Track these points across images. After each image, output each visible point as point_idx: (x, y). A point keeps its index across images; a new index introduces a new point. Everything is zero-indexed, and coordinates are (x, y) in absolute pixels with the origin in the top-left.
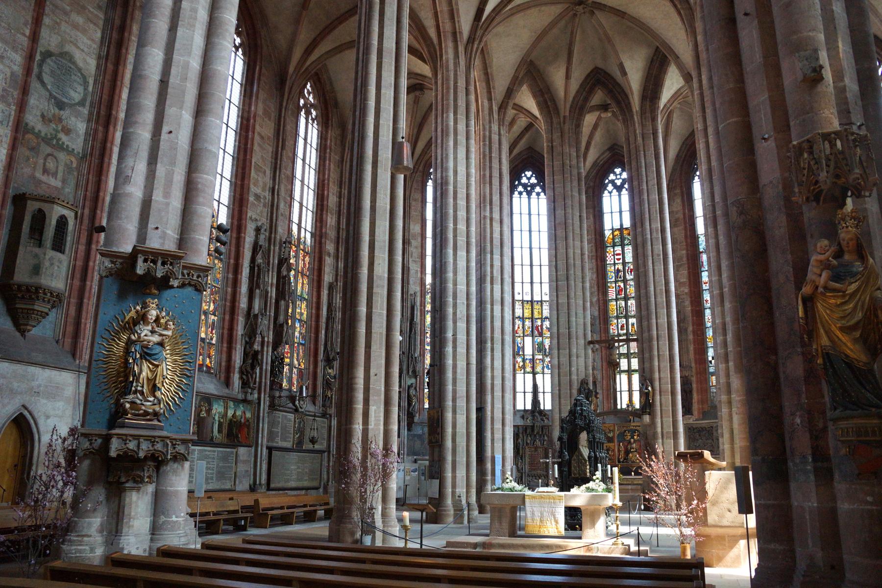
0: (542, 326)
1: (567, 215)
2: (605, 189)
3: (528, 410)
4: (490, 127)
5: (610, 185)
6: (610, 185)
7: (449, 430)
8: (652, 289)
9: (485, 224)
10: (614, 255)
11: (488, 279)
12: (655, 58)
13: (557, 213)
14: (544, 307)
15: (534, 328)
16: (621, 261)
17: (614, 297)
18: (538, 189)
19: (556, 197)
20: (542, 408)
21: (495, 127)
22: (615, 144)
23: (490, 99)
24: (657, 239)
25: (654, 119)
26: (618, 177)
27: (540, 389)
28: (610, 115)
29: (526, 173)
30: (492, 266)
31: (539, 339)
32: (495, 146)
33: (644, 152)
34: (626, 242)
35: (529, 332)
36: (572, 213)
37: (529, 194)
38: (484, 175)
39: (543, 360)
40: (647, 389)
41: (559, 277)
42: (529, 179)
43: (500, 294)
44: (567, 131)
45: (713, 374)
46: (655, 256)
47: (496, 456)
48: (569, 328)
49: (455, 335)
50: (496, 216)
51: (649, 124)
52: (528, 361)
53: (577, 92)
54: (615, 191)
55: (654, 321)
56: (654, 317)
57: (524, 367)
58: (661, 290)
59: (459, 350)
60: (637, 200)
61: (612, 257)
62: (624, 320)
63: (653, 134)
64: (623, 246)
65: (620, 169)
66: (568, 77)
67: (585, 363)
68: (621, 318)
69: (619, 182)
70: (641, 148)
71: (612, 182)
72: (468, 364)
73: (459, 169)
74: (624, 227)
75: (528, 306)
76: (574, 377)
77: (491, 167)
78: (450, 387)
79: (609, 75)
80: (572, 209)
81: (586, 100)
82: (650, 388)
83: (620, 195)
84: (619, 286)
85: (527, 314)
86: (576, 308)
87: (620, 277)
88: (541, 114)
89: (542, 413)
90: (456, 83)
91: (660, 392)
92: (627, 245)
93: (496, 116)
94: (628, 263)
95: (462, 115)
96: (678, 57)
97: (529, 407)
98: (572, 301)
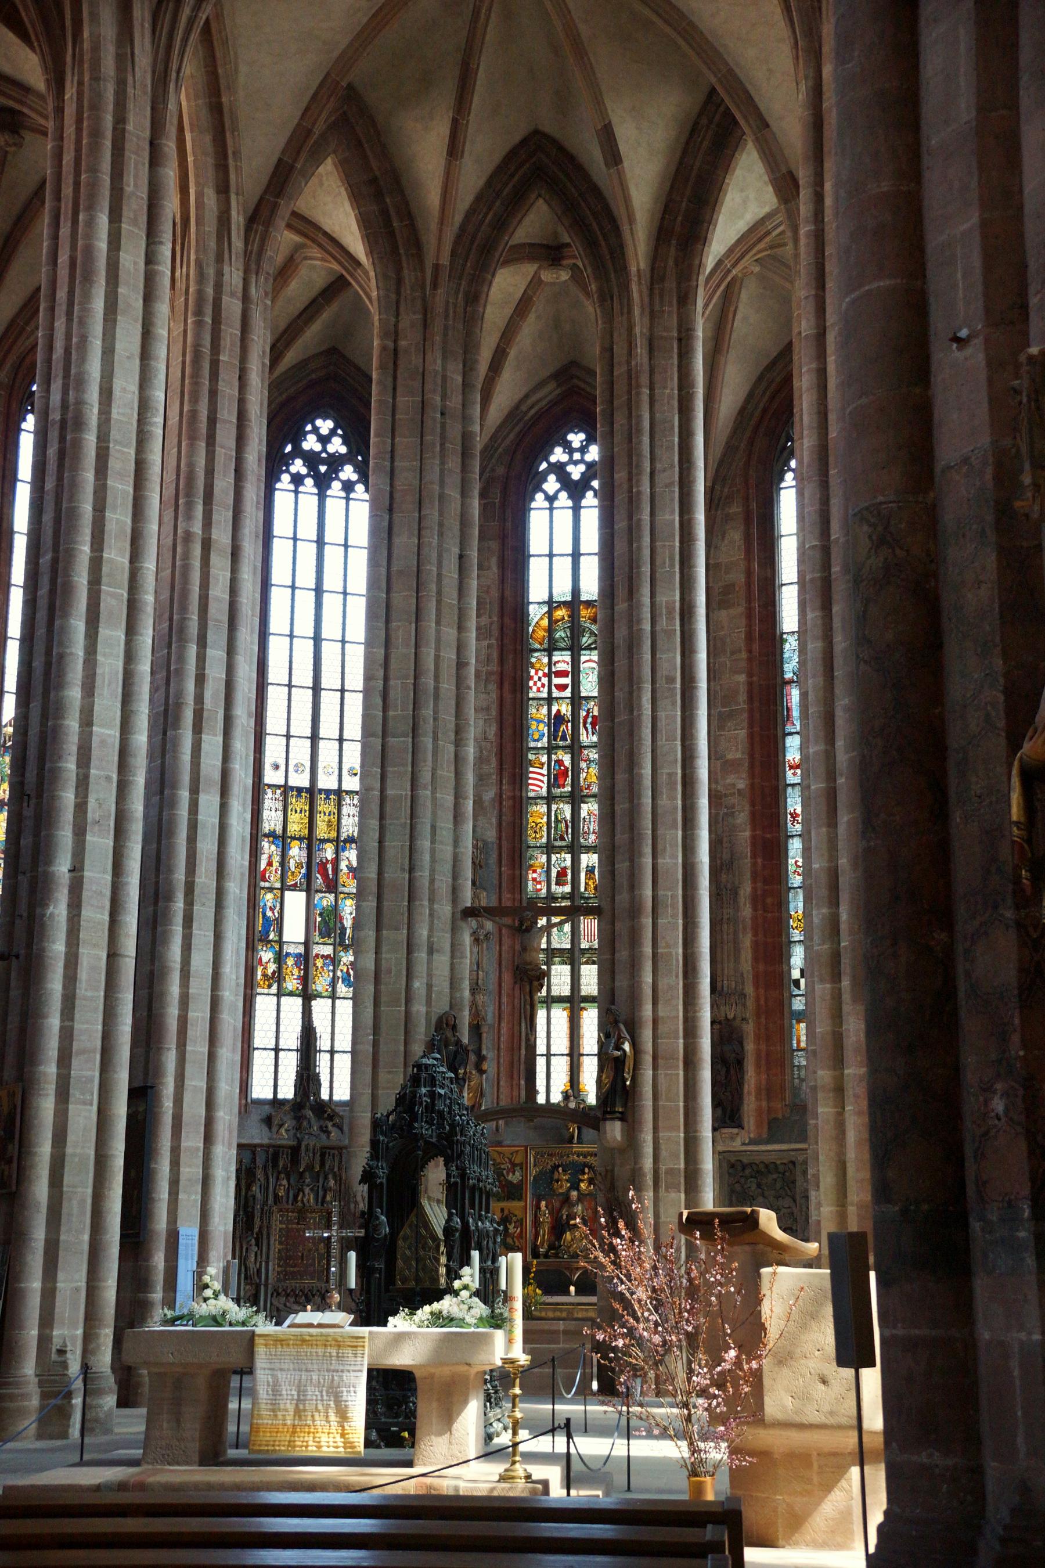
0: (336, 861)
1: (425, 551)
2: (538, 488)
3: (284, 1102)
4: (220, 274)
5: (552, 478)
6: (552, 478)
7: (44, 1149)
8: (647, 771)
9: (186, 556)
10: (549, 675)
11: (188, 715)
12: (704, 121)
13: (396, 541)
14: (345, 810)
15: (315, 868)
16: (568, 693)
17: (544, 792)
18: (348, 473)
19: (397, 496)
20: (325, 1095)
21: (234, 277)
22: (574, 364)
23: (223, 189)
24: (670, 633)
25: (685, 299)
26: (577, 456)
27: (323, 1043)
28: (564, 276)
29: (319, 422)
30: (201, 679)
31: (327, 900)
32: (231, 332)
33: (652, 389)
34: (585, 640)
35: (297, 876)
36: (440, 545)
37: (322, 484)
38: (194, 414)
39: (334, 960)
40: (618, 1047)
41: (391, 723)
42: (324, 440)
43: (219, 763)
44: (439, 309)
45: (800, 1017)
46: (661, 683)
47: (183, 1231)
48: (411, 870)
49: (77, 869)
50: (222, 536)
51: (670, 311)
52: (290, 961)
53: (479, 198)
54: (563, 495)
55: (648, 860)
56: (648, 850)
57: (278, 977)
58: (671, 775)
59: (86, 913)
60: (621, 525)
61: (545, 680)
62: (568, 857)
63: (680, 340)
64: (575, 650)
65: (582, 436)
66: (454, 150)
67: (452, 965)
68: (559, 850)
69: (576, 472)
70: (644, 379)
71: (559, 469)
72: (113, 955)
73: (118, 384)
74: (583, 598)
75: (299, 804)
76: (419, 1008)
77: (213, 393)
78: (54, 1022)
79: (571, 158)
80: (441, 534)
81: (502, 225)
82: (627, 1047)
83: (576, 509)
84: (560, 762)
85: (297, 825)
86: (434, 814)
87: (564, 738)
88: (371, 252)
89: (326, 1111)
90: (120, 120)
91: (655, 1058)
92: (589, 648)
93: (238, 244)
94: (587, 698)
95: (135, 222)
96: (767, 126)
97: (287, 1091)
98: (425, 793)
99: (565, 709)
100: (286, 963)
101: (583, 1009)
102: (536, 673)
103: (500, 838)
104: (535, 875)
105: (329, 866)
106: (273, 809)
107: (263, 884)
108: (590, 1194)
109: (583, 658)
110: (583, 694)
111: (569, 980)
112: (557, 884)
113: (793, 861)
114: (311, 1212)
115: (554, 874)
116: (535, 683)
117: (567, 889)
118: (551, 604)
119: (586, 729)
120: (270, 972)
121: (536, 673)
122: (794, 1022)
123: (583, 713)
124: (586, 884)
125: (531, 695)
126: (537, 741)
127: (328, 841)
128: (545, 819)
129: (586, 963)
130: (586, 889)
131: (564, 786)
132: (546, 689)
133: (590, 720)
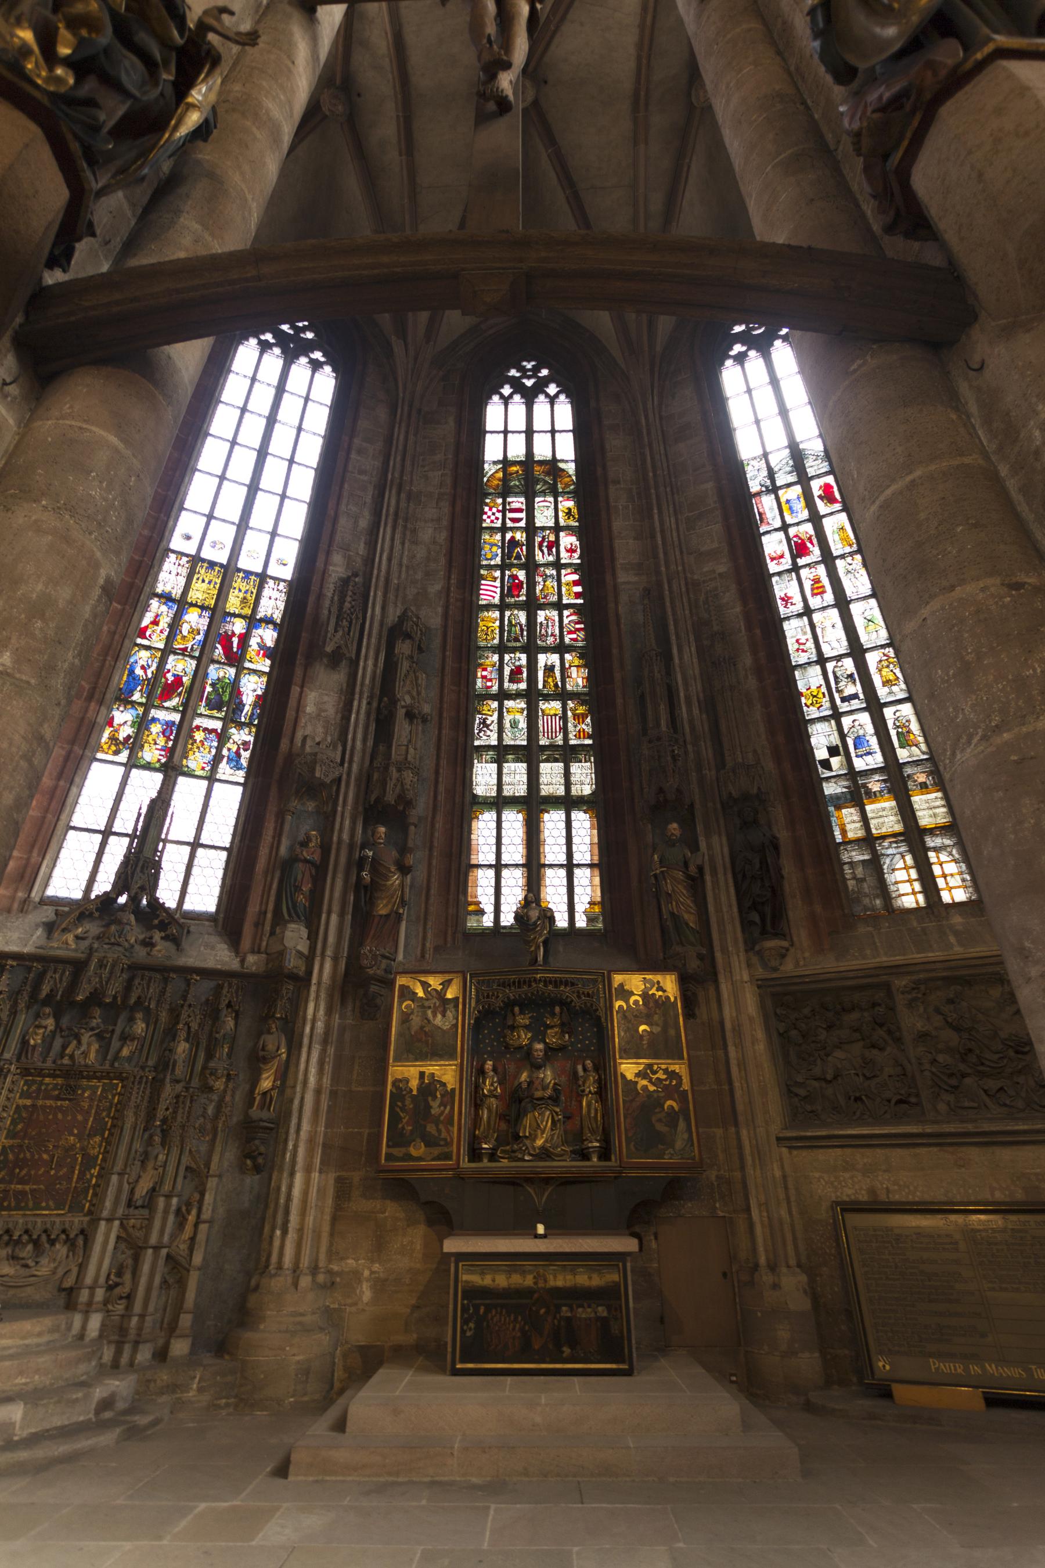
0: (244, 638)
16: (523, 524)
17: (497, 601)
39: (222, 737)
45: (839, 802)
52: (156, 728)
57: (134, 744)
68: (513, 650)
84: (516, 577)
87: (518, 557)
92: (544, 493)
94: (543, 528)
99: (520, 536)
100: (148, 729)
102: (490, 509)
103: (445, 627)
104: (485, 673)
105: (235, 640)
106: (174, 573)
107: (139, 641)
108: (562, 1048)
109: (537, 500)
110: (538, 524)
111: (525, 778)
112: (510, 681)
113: (794, 640)
114: (89, 1078)
115: (507, 671)
116: (489, 517)
117: (523, 686)
118: (506, 463)
119: (542, 551)
120: (122, 736)
121: (490, 509)
123: (538, 539)
124: (544, 681)
125: (484, 525)
126: (491, 559)
127: (239, 616)
128: (498, 623)
129: (547, 761)
130: (544, 686)
131: (518, 596)
132: (500, 521)
133: (545, 544)
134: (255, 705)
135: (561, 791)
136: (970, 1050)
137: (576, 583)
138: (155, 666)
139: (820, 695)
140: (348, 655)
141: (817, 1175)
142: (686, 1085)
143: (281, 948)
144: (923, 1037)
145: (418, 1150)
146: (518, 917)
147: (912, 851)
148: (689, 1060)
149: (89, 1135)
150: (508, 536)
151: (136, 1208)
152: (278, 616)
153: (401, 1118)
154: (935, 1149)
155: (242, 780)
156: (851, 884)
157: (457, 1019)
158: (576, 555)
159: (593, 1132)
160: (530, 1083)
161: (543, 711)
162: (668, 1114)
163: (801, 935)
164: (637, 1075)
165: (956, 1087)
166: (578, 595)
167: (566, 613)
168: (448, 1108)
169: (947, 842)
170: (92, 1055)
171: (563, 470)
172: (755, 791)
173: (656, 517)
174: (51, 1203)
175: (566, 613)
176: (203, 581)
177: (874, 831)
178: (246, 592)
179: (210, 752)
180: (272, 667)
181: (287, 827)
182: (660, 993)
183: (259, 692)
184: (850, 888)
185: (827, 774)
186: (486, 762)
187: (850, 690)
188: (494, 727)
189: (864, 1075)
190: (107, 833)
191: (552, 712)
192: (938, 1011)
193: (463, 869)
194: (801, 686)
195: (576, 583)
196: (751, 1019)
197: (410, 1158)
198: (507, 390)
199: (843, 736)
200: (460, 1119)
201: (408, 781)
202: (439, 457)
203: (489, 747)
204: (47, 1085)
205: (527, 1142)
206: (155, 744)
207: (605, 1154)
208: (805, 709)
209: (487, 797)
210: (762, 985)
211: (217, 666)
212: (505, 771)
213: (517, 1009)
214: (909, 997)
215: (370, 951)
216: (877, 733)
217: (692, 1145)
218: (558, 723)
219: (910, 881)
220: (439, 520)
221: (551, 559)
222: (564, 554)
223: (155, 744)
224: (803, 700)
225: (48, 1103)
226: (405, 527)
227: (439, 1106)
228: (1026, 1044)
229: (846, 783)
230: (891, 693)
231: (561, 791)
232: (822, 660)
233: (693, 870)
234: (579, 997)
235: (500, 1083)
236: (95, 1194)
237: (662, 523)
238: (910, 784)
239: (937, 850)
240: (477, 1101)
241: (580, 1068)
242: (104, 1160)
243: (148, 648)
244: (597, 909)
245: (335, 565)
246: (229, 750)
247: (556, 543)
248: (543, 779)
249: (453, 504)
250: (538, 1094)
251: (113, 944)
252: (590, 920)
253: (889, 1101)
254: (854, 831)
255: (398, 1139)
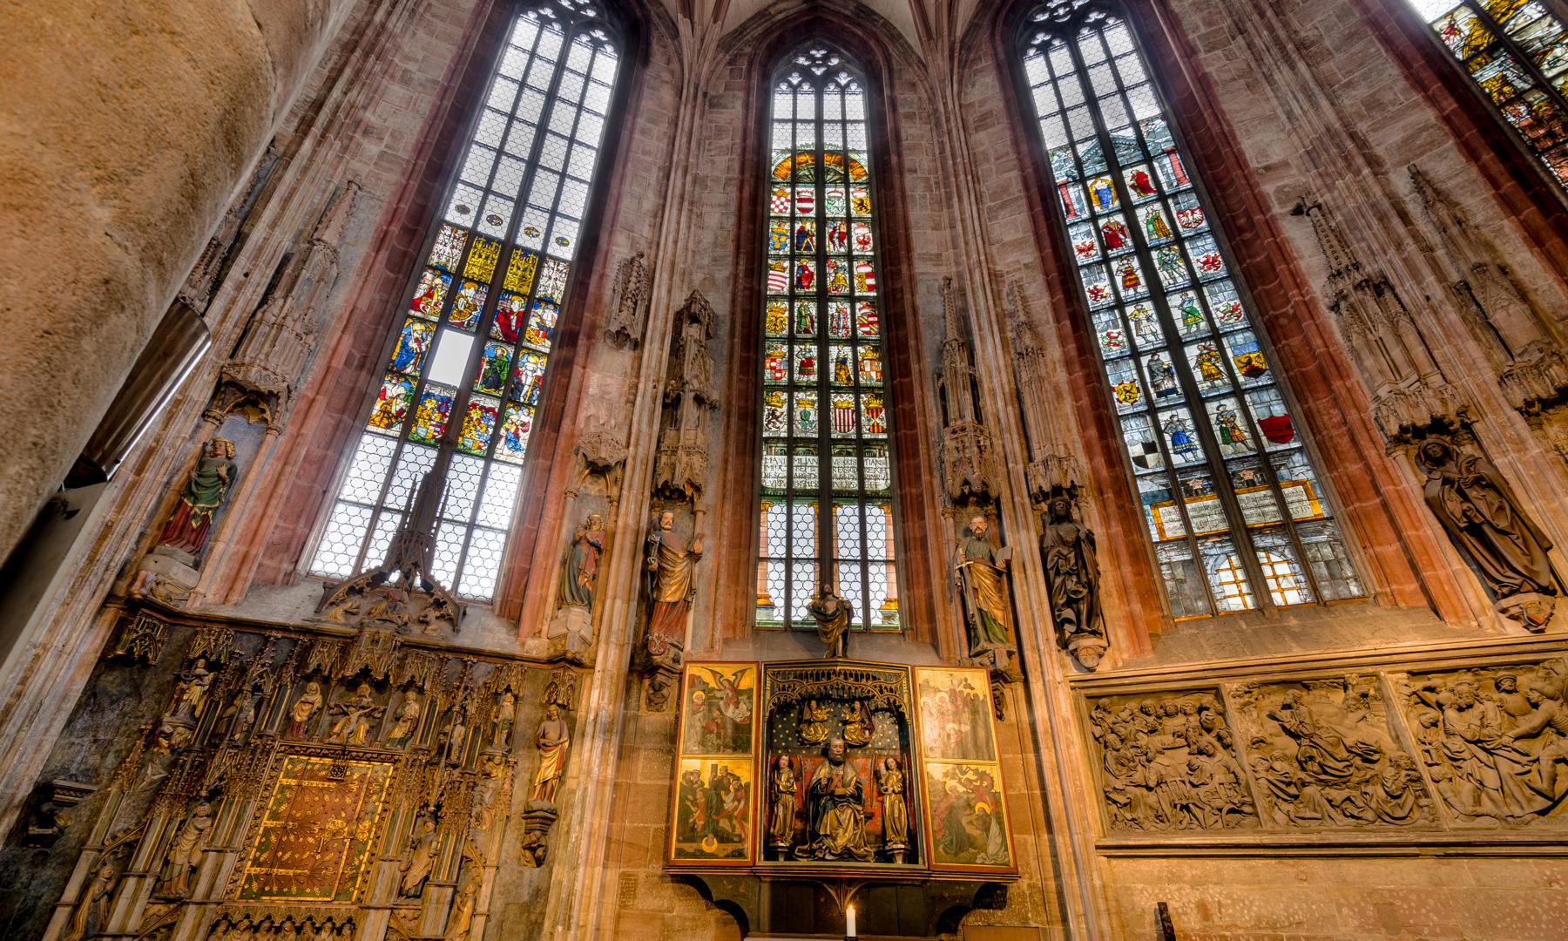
0: (523, 318)
16: (812, 214)
17: (786, 291)
39: (500, 417)
52: (430, 404)
57: (408, 419)
61: (788, 205)
68: (804, 341)
84: (804, 268)
87: (808, 248)
94: (834, 219)
101: (834, 505)
102: (779, 198)
103: (733, 313)
104: (773, 364)
105: (514, 319)
107: (412, 312)
109: (827, 190)
111: (816, 472)
113: (1104, 334)
117: (814, 378)
120: (394, 409)
121: (779, 198)
122: (1147, 507)
127: (518, 294)
128: (787, 314)
129: (839, 454)
130: (836, 379)
131: (808, 287)
134: (534, 386)
135: (854, 485)
136: (1312, 758)
137: (868, 275)
138: (429, 339)
139: (1134, 390)
140: (633, 336)
141: (1140, 886)
142: (998, 787)
143: (565, 630)
144: (1258, 743)
145: (710, 845)
146: (814, 610)
147: (1237, 551)
148: (1001, 761)
149: (358, 819)
150: (798, 226)
151: (409, 897)
152: (558, 297)
153: (692, 813)
154: (1273, 861)
155: (521, 462)
156: (1170, 585)
157: (751, 711)
158: (869, 247)
159: (897, 833)
160: (830, 780)
161: (835, 404)
162: (979, 817)
163: (1118, 634)
164: (946, 775)
165: (1296, 797)
166: (870, 288)
167: (858, 305)
168: (743, 803)
169: (1279, 542)
170: (362, 734)
171: (855, 161)
172: (1069, 485)
173: (956, 205)
174: (316, 889)
175: (858, 305)
176: (480, 256)
177: (1196, 530)
178: (525, 270)
179: (487, 431)
180: (552, 348)
181: (568, 509)
182: (968, 690)
183: (539, 373)
184: (1169, 589)
185: (1142, 471)
186: (776, 454)
187: (1168, 385)
188: (784, 418)
189: (1191, 783)
190: (379, 508)
191: (845, 405)
192: (1272, 717)
193: (752, 562)
194: (1112, 381)
195: (868, 275)
196: (1066, 722)
197: (701, 853)
198: (795, 79)
199: (1159, 433)
200: (755, 816)
201: (697, 466)
202: (726, 142)
203: (778, 439)
204: (313, 764)
205: (828, 842)
206: (430, 419)
207: (911, 856)
208: (1117, 404)
209: (776, 490)
210: (1076, 685)
211: (495, 343)
212: (796, 463)
213: (814, 703)
214: (1242, 701)
215: (659, 638)
216: (1198, 429)
217: (1006, 850)
218: (850, 417)
219: (1236, 582)
220: (726, 205)
221: (842, 250)
222: (855, 246)
223: (430, 419)
224: (1115, 395)
225: (315, 783)
226: (691, 211)
227: (733, 801)
228: (1376, 752)
229: (1164, 481)
230: (1213, 387)
231: (854, 485)
232: (1135, 354)
233: (1000, 565)
234: (881, 692)
235: (797, 779)
236: (365, 882)
237: (962, 213)
238: (1236, 482)
239: (1265, 549)
240: (772, 798)
241: (882, 766)
242: (374, 844)
243: (422, 321)
244: (894, 607)
245: (619, 246)
246: (507, 430)
247: (849, 234)
248: (836, 473)
249: (741, 189)
250: (839, 791)
251: (385, 620)
252: (888, 617)
253: (1220, 810)
254: (1174, 529)
255: (689, 834)
